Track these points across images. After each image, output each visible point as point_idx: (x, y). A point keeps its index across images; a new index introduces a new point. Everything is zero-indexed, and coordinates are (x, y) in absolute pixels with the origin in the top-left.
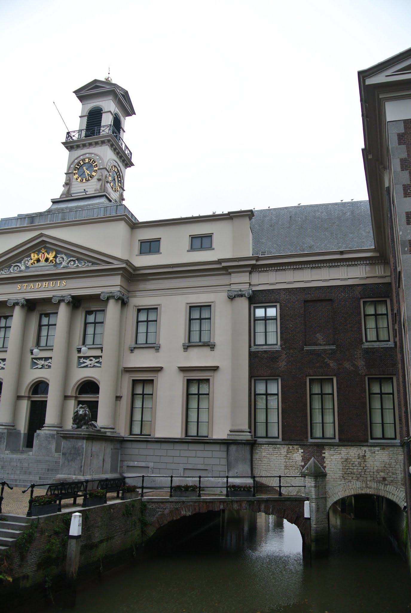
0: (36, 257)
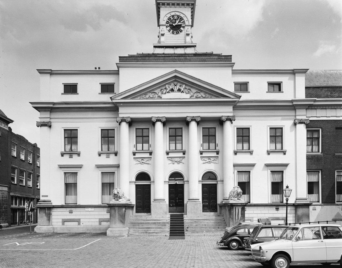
0: (171, 88)
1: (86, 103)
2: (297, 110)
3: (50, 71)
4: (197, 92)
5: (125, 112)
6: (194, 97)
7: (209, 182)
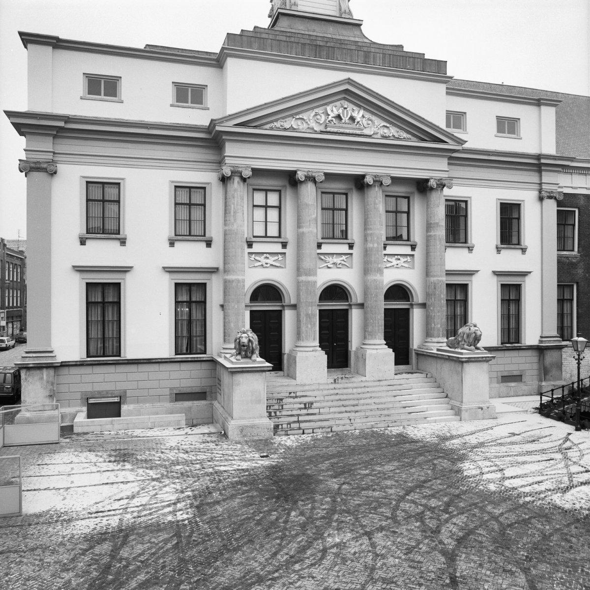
0: (336, 113)
1: (137, 125)
2: (543, 173)
3: (55, 41)
4: (384, 126)
5: (239, 155)
6: (379, 136)
7: (401, 304)
